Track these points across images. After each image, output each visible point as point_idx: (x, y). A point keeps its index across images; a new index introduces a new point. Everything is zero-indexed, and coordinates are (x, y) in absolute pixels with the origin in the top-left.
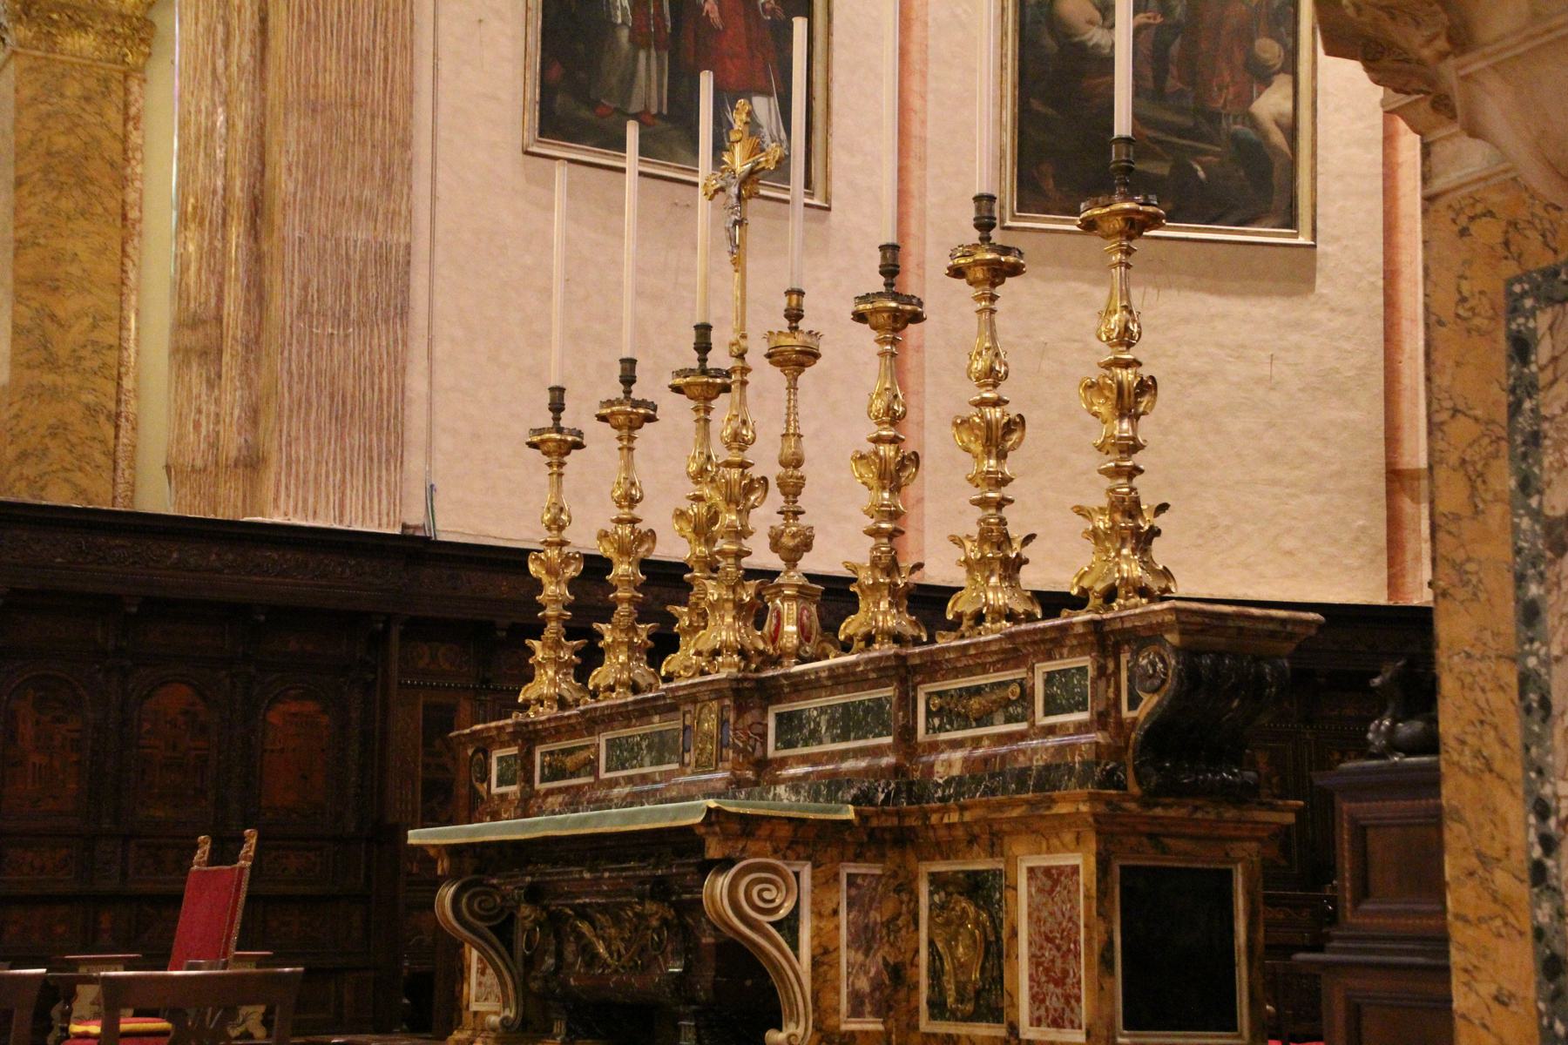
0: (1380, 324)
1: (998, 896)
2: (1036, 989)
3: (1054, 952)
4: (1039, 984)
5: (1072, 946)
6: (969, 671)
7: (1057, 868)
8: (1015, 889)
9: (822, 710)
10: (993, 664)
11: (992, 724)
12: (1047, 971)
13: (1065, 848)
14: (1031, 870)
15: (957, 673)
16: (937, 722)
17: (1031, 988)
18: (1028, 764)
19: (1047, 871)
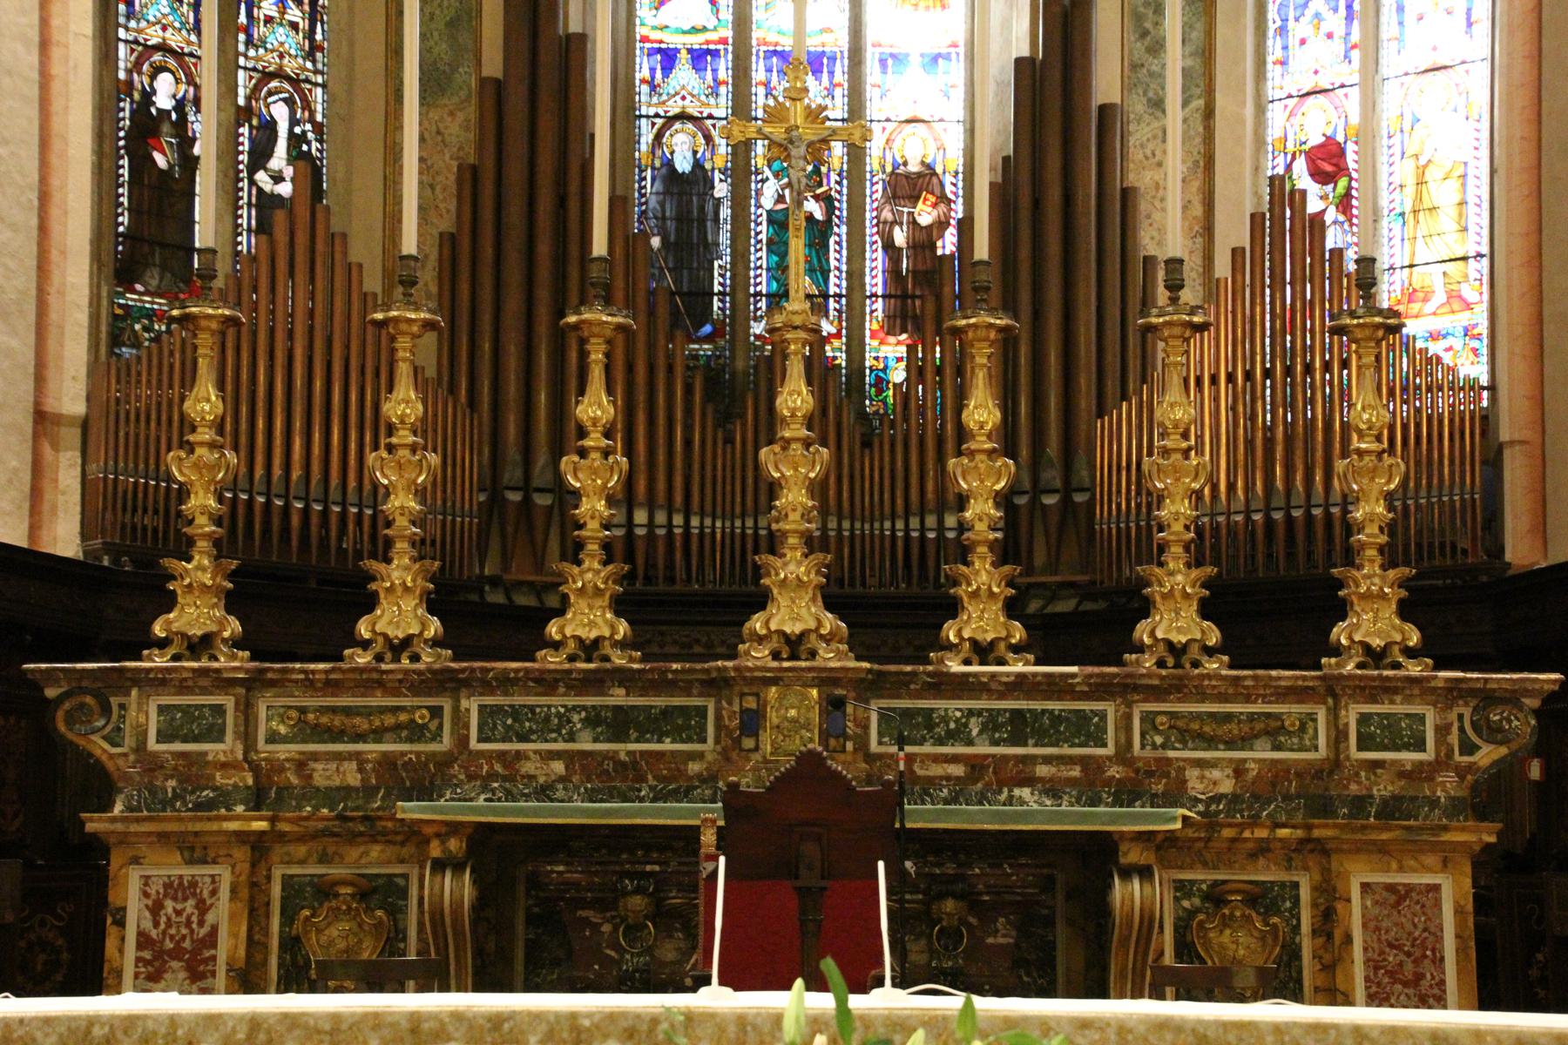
0: (35, 248)
1: (1288, 904)
2: (1374, 989)
3: (1402, 957)
4: (1379, 984)
5: (1428, 953)
6: (1223, 698)
7: (1405, 885)
8: (1349, 900)
10: (1264, 696)
11: (1252, 749)
12: (1391, 974)
13: (1429, 870)
14: (1365, 887)
15: (1203, 697)
16: (1159, 740)
17: (1367, 988)
18: (1364, 792)
19: (1390, 888)
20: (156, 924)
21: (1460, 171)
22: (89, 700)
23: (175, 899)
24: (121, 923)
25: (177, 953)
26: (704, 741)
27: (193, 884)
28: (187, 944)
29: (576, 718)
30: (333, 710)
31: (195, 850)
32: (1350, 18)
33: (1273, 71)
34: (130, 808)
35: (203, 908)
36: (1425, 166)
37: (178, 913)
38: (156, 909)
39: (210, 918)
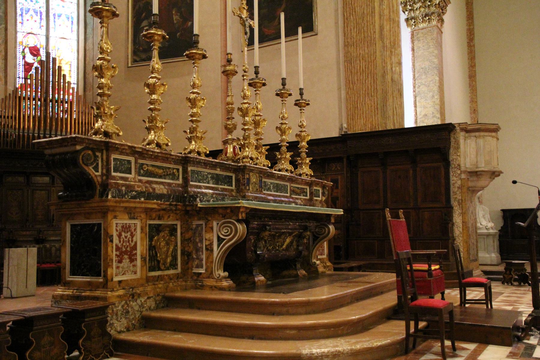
9: (271, 183)
20: (120, 242)
21: (70, 63)
22: (90, 152)
23: (125, 232)
24: (112, 241)
25: (126, 252)
26: (232, 186)
27: (130, 227)
28: (128, 249)
29: (209, 176)
30: (153, 166)
31: (131, 213)
32: (41, 19)
33: (19, 25)
34: (113, 197)
35: (132, 236)
36: (61, 60)
37: (126, 237)
38: (120, 236)
39: (134, 239)
